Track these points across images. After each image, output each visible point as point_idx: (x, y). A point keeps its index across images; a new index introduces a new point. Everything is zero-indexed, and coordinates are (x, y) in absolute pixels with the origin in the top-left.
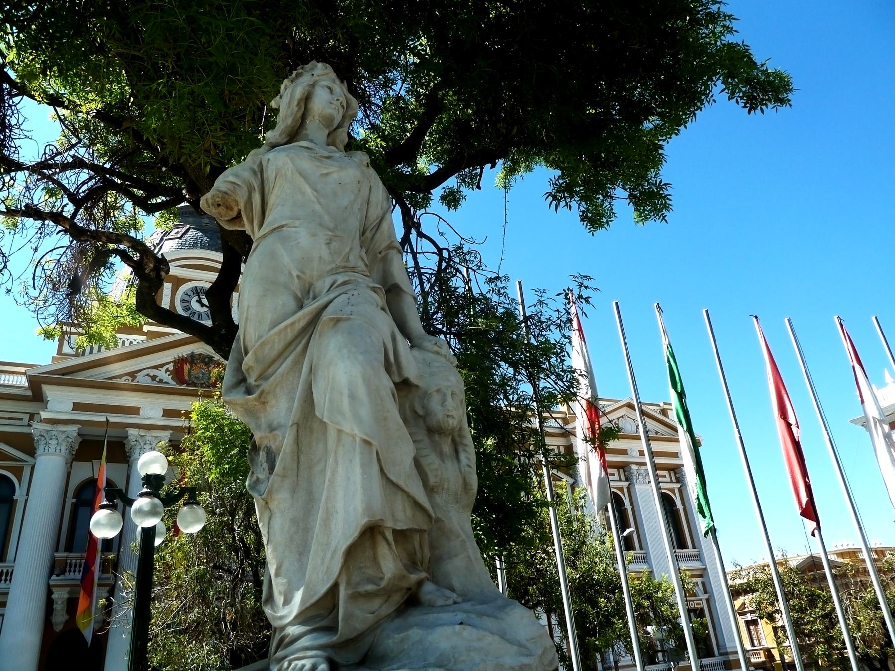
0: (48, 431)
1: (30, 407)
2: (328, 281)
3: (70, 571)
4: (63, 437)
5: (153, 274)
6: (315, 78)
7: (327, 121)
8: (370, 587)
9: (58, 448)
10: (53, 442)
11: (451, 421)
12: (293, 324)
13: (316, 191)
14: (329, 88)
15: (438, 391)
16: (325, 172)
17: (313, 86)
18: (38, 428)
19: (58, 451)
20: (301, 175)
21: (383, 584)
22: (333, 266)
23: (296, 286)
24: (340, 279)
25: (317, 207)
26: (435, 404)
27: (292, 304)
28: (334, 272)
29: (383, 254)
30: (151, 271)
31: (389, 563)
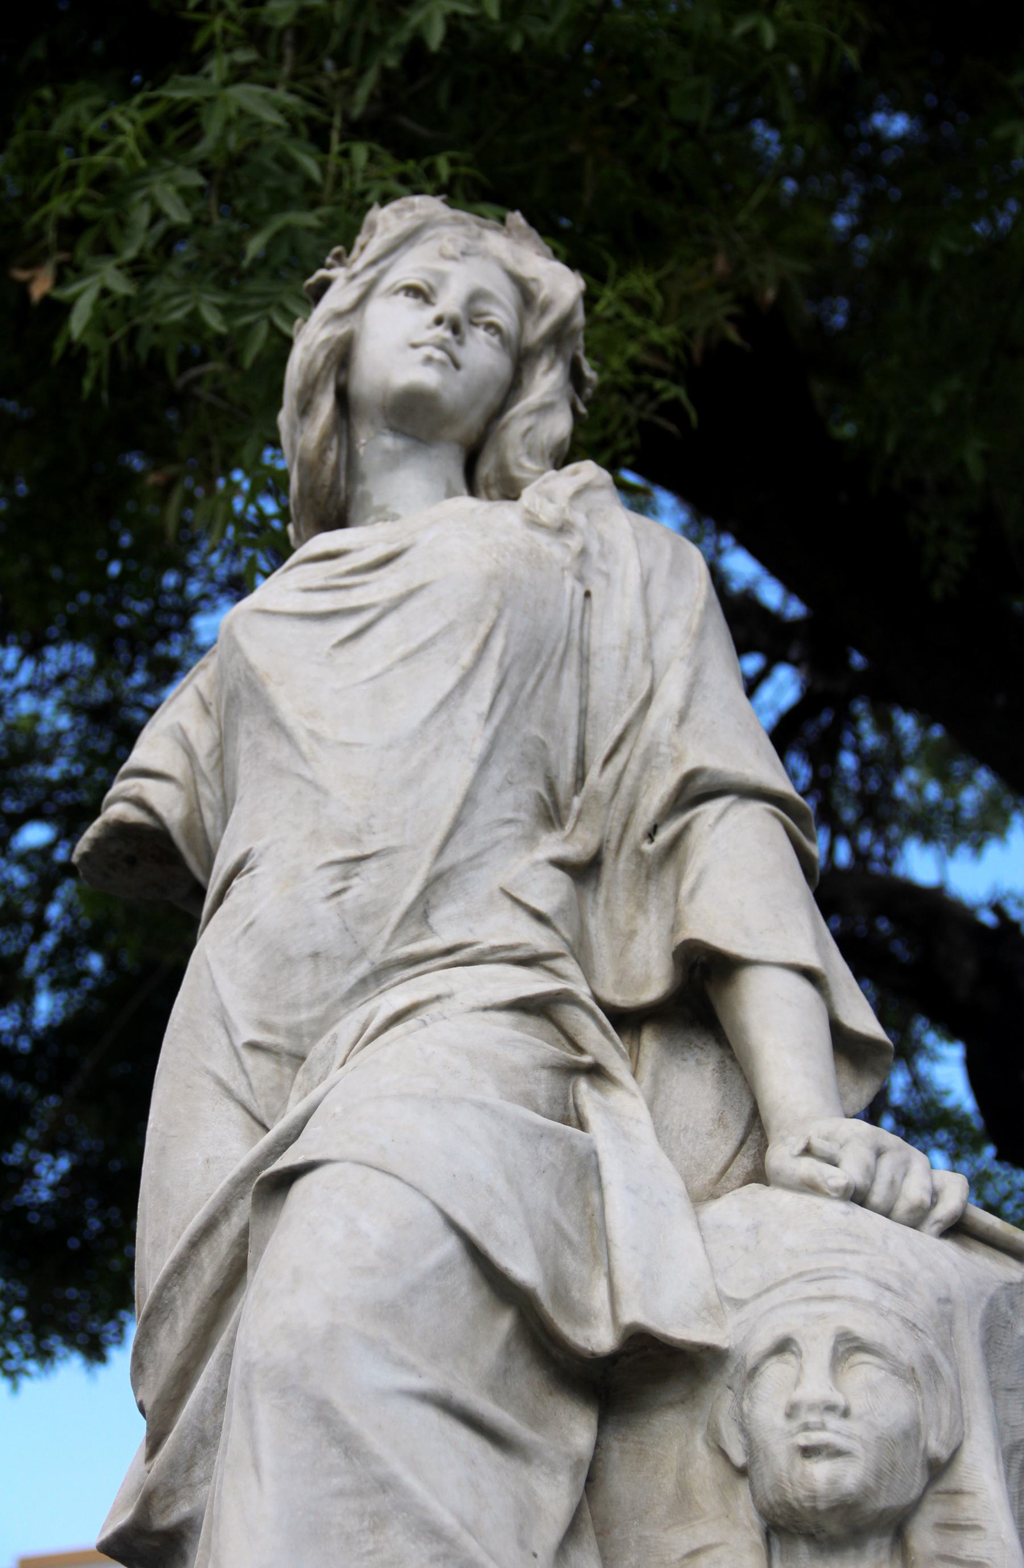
12: (208, 1229)
14: (414, 291)
22: (362, 969)
29: (664, 835)
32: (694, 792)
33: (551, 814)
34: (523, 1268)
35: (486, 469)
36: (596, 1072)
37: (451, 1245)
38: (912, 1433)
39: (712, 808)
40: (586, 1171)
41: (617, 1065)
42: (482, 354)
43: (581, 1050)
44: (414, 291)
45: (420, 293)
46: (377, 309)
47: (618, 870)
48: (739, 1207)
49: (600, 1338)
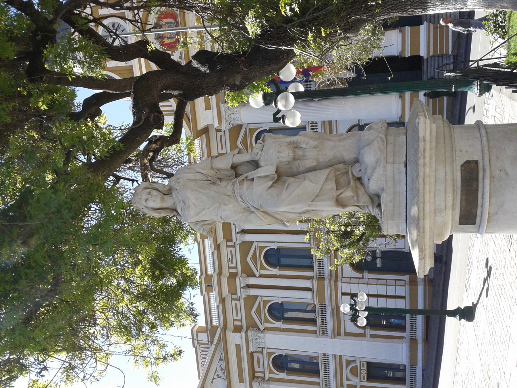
0: (226, 121)
1: (212, 133)
2: (242, 203)
3: (310, 87)
4: (228, 111)
5: (159, 143)
6: (143, 207)
7: (163, 199)
8: (355, 198)
9: (236, 113)
10: (232, 116)
11: (290, 155)
12: (262, 216)
13: (204, 209)
14: (146, 201)
15: (278, 158)
16: (193, 206)
17: (147, 207)
18: (225, 127)
19: (238, 112)
20: (198, 215)
21: (354, 195)
23: (246, 214)
24: (240, 199)
25: (211, 209)
26: (285, 160)
27: (253, 215)
28: (237, 200)
30: (157, 145)
31: (348, 194)
32: (212, 168)
33: (214, 183)
34: (271, 183)
35: (166, 193)
36: (246, 177)
37: (269, 190)
38: (286, 146)
39: (214, 167)
40: (260, 177)
41: (246, 175)
42: (155, 193)
43: (244, 179)
44: (146, 201)
45: (147, 200)
46: (148, 206)
47: (220, 176)
48: (262, 163)
49: (276, 176)
